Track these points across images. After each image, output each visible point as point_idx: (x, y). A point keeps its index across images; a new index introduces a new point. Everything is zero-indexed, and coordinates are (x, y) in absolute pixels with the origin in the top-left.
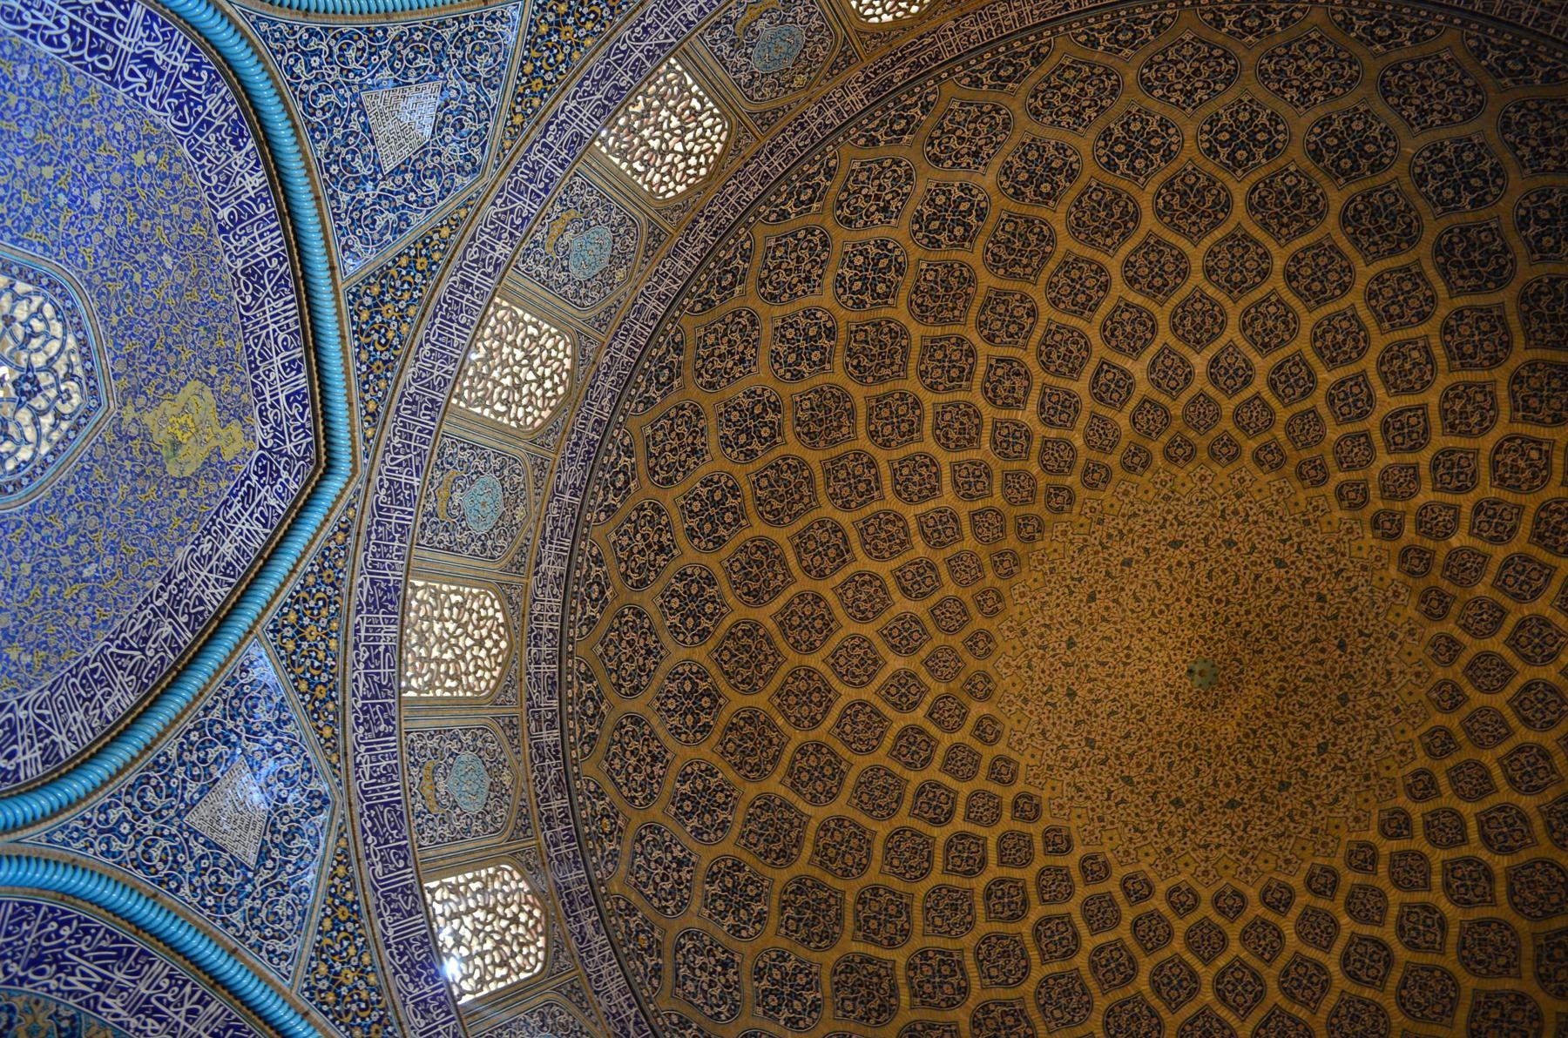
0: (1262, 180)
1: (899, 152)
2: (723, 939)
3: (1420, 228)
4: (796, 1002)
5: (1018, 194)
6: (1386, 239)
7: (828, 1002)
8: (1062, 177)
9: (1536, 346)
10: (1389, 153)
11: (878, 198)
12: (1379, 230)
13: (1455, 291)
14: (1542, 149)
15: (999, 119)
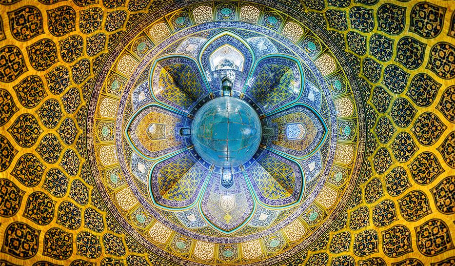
0: (419, 140)
1: (344, 230)
2: (113, 256)
3: (416, 76)
4: (86, 241)
5: (383, 224)
6: (427, 85)
7: (74, 240)
8: (391, 209)
9: (402, 8)
10: (400, 101)
11: (341, 243)
12: (425, 89)
13: (424, 46)
14: (375, 69)
15: (364, 210)
